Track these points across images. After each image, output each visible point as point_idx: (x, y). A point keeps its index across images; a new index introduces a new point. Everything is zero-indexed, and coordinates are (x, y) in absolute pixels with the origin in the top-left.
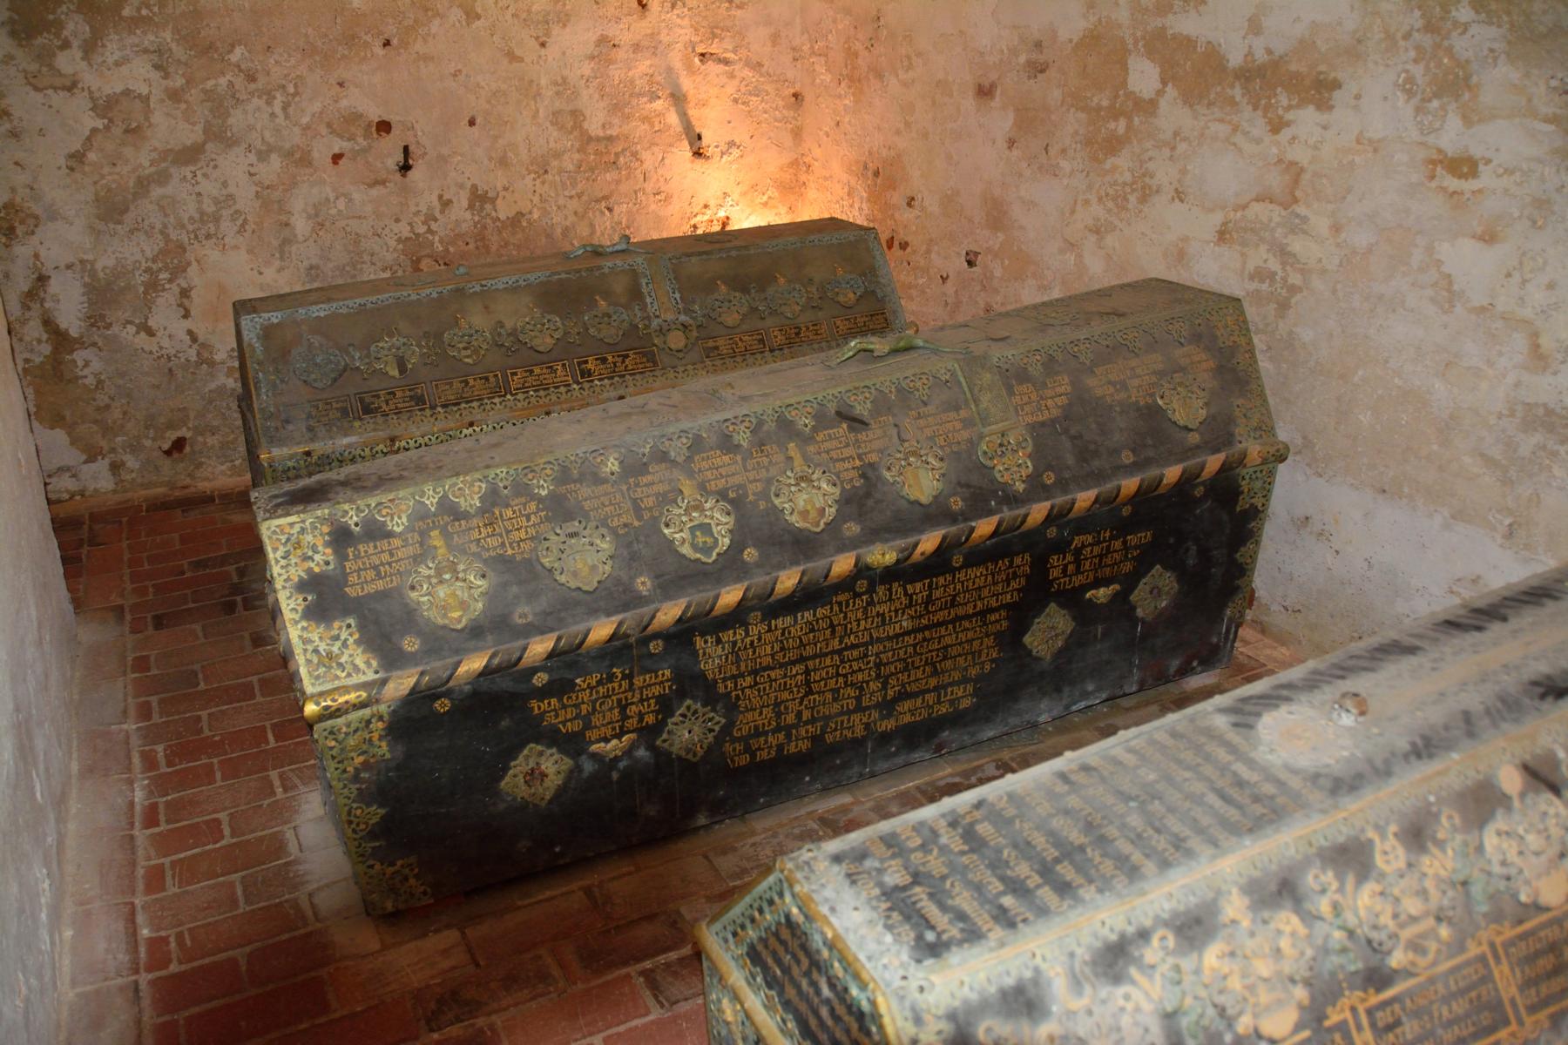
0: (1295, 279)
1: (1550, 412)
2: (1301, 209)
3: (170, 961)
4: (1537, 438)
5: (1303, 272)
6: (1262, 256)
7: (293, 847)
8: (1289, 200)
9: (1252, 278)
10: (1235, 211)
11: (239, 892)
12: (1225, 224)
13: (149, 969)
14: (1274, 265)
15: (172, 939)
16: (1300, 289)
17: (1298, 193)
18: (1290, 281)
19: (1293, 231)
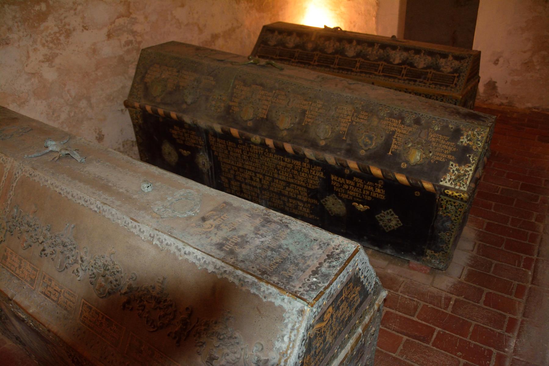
0: (139, 39)
2: (133, 16)
3: (525, 259)
6: (126, 37)
7: (465, 272)
8: (128, 14)
9: (124, 46)
10: (111, 25)
11: (492, 269)
12: (109, 31)
13: (532, 260)
14: (131, 38)
15: (522, 266)
17: (131, 11)
18: (138, 40)
19: (133, 24)
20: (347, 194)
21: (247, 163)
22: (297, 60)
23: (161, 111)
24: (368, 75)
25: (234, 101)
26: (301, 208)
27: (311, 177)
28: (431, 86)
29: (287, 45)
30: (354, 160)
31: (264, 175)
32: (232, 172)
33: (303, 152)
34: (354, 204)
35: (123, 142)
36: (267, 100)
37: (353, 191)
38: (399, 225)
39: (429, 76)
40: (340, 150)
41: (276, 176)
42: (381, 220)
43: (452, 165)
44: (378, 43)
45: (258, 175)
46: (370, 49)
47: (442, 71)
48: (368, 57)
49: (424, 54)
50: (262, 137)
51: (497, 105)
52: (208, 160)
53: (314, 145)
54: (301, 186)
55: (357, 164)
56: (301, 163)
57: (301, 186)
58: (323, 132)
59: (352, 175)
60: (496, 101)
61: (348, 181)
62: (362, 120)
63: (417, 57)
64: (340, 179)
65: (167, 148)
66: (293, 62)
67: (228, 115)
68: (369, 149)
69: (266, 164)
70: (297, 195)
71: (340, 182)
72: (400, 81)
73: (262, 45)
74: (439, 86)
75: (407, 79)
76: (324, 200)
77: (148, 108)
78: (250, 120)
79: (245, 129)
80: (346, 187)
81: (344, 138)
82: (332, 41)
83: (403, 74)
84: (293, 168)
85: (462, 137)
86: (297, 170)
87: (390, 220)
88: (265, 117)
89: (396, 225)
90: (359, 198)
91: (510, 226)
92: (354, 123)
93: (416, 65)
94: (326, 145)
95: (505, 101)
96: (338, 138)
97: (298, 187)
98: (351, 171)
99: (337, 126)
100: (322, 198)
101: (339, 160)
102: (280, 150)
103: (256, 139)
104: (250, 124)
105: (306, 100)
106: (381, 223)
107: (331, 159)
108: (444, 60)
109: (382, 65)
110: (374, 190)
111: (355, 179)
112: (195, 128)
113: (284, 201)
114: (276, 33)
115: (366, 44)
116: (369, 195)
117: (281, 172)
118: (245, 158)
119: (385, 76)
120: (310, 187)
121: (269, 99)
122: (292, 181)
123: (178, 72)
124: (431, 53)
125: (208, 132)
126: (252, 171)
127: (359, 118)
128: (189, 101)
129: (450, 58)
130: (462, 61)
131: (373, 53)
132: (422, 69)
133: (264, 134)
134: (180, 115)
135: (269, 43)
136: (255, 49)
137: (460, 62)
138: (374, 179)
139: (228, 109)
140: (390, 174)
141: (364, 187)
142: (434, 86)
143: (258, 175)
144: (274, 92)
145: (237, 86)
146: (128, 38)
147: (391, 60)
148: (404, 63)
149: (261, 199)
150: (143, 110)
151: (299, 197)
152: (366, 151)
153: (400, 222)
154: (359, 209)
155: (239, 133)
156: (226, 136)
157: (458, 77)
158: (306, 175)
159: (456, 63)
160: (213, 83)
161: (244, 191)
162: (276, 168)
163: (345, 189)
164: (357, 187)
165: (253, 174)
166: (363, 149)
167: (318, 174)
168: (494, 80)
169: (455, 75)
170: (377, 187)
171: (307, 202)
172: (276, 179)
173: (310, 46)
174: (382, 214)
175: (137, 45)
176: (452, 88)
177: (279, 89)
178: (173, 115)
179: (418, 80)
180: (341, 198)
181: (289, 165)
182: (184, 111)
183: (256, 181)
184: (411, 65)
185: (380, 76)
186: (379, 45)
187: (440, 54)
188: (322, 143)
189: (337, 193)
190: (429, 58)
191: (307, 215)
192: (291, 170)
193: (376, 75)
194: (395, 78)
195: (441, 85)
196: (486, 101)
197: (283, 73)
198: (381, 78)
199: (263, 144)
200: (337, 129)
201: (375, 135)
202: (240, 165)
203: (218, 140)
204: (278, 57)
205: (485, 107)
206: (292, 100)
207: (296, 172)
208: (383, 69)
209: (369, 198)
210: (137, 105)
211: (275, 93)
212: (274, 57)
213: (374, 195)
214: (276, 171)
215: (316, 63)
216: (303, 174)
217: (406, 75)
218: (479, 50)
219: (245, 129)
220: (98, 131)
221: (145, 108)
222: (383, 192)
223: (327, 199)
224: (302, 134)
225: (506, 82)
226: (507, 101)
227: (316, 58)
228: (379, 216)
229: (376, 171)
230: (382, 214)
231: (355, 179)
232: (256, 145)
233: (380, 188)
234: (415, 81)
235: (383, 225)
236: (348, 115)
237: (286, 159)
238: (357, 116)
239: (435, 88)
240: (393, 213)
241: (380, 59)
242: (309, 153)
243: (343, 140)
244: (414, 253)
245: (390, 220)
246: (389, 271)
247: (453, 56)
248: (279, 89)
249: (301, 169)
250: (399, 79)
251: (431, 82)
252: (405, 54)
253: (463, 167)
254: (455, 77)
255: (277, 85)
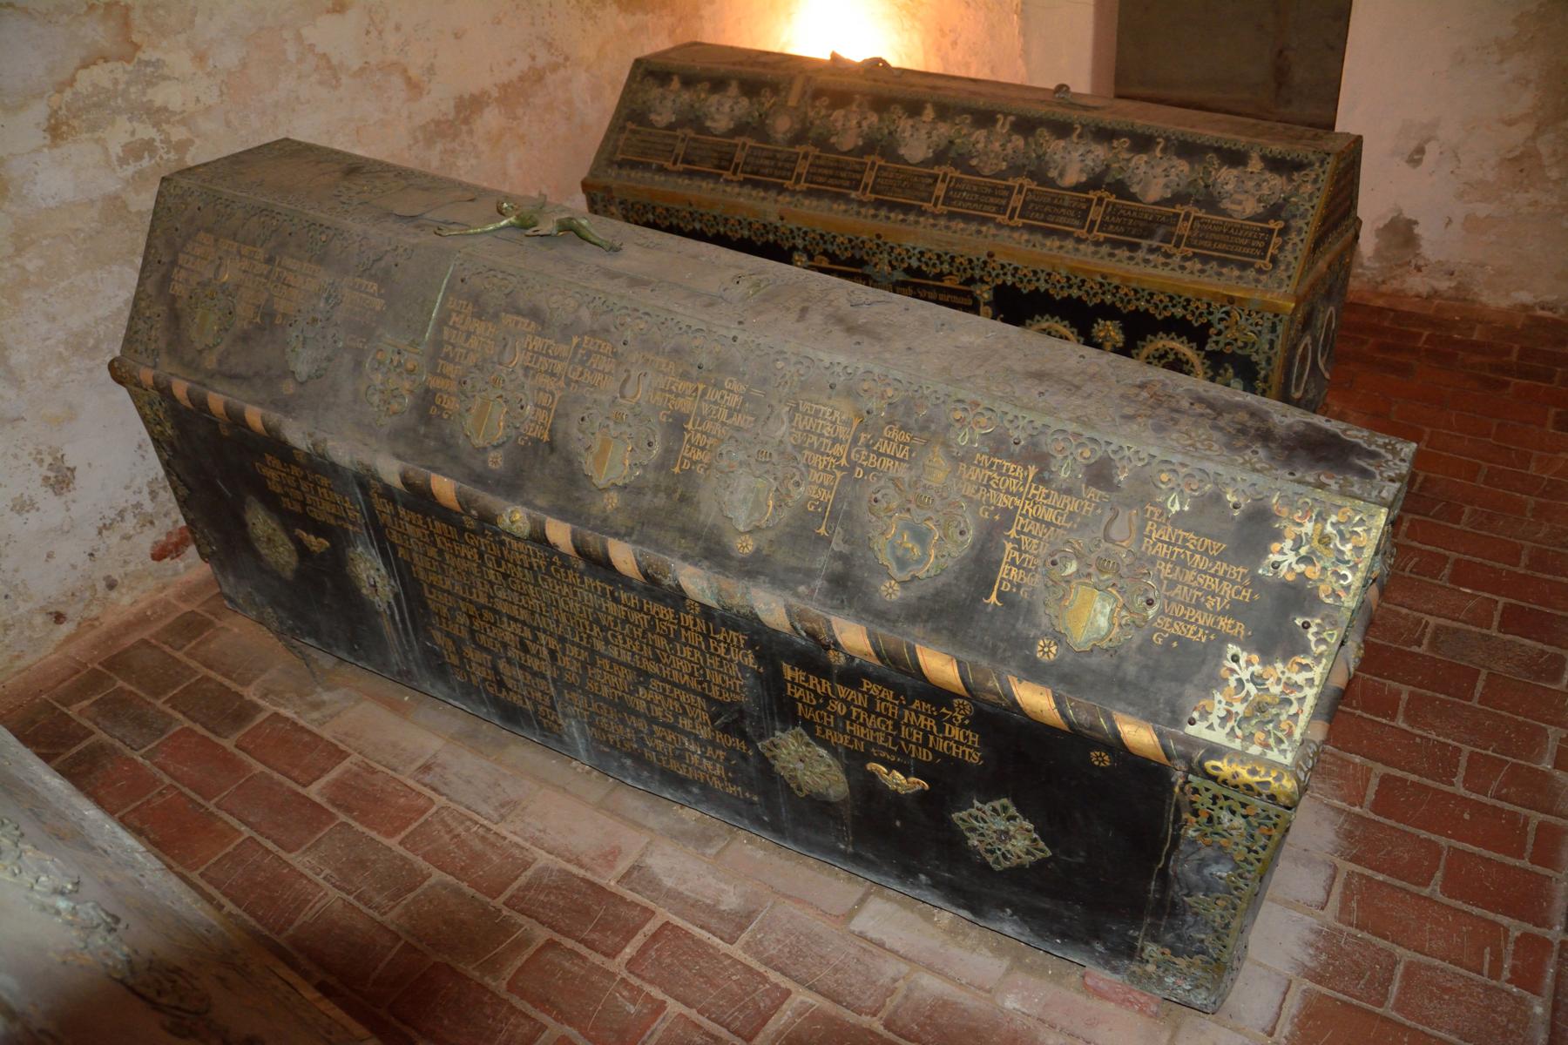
0: (178, 134)
1: (438, 123)
2: (146, 55)
3: (1518, 940)
4: (439, 147)
5: (183, 122)
6: (119, 134)
7: (1293, 1005)
8: (129, 50)
9: (123, 161)
10: (60, 92)
11: (1395, 988)
12: (54, 113)
14: (146, 132)
15: (1506, 974)
16: (190, 142)
17: (136, 38)
18: (174, 139)
19: (150, 84)
20: (844, 732)
21: (501, 594)
22: (740, 176)
23: (216, 401)
24: (973, 227)
25: (445, 376)
26: (695, 759)
27: (715, 662)
28: (1188, 264)
29: (708, 123)
30: (859, 620)
31: (562, 640)
32: (463, 619)
33: (675, 579)
34: (872, 766)
35: (150, 484)
36: (553, 375)
37: (864, 725)
38: (1040, 855)
39: (1183, 228)
40: (810, 574)
41: (600, 646)
42: (973, 830)
43: (1235, 659)
44: (1006, 115)
45: (542, 636)
46: (980, 134)
47: (1224, 212)
48: (974, 162)
49: (1164, 150)
50: (536, 514)
51: (1418, 296)
52: (383, 571)
53: (714, 553)
54: (684, 687)
55: (870, 635)
56: (676, 613)
57: (684, 687)
58: (743, 504)
59: (853, 675)
60: (1417, 284)
61: (842, 691)
62: (887, 462)
63: (1141, 160)
64: (813, 680)
65: (260, 522)
66: (728, 182)
67: (426, 422)
68: (914, 578)
69: (561, 604)
70: (676, 716)
71: (815, 692)
72: (1082, 247)
73: (630, 125)
74: (1214, 264)
75: (1107, 240)
76: (767, 743)
77: (180, 389)
78: (495, 447)
79: (479, 479)
80: (840, 709)
81: (822, 531)
82: (854, 108)
83: (1093, 223)
84: (652, 628)
85: (1276, 546)
86: (666, 636)
87: (1005, 835)
88: (546, 437)
89: (1028, 853)
90: (890, 752)
91: (1462, 791)
92: (859, 473)
93: (1135, 189)
94: (758, 550)
95: (1444, 285)
96: (802, 532)
97: (677, 691)
98: (851, 658)
99: (798, 484)
100: (761, 737)
101: (801, 615)
102: (601, 565)
103: (515, 518)
104: (496, 461)
105: (685, 376)
106: (974, 841)
107: (771, 608)
108: (1235, 172)
109: (1020, 192)
110: (941, 729)
111: (866, 685)
112: (318, 467)
113: (637, 731)
114: (676, 84)
115: (968, 119)
116: (925, 744)
117: (614, 636)
118: (492, 578)
119: (1032, 229)
120: (715, 693)
121: (559, 367)
122: (653, 668)
123: (270, 260)
124: (1188, 150)
125: (365, 481)
126: (524, 623)
127: (880, 455)
128: (302, 368)
129: (1255, 165)
130: (1295, 176)
131: (994, 148)
132: (1155, 203)
133: (540, 502)
134: (275, 417)
135: (653, 117)
136: (607, 138)
137: (1291, 180)
138: (938, 696)
139: (427, 401)
140: (994, 684)
141: (901, 717)
142: (1199, 266)
143: (542, 636)
144: (575, 340)
145: (454, 318)
146: (133, 133)
147: (1053, 174)
148: (1094, 182)
149: (565, 715)
150: (165, 391)
151: (685, 723)
152: (902, 583)
153: (1042, 844)
154: (892, 787)
155: (459, 494)
156: (419, 498)
157: (1284, 232)
158: (697, 654)
159: (1275, 184)
160: (379, 304)
161: (510, 683)
162: (597, 621)
163: (835, 714)
164: (879, 715)
165: (527, 634)
166: (892, 578)
167: (736, 657)
168: (1408, 215)
169: (1272, 225)
170: (950, 721)
171: (712, 742)
172: (603, 656)
173: (782, 125)
174: (973, 811)
175: (173, 156)
176: (1260, 271)
177: (593, 333)
178: (254, 416)
179: (1145, 243)
180: (824, 743)
181: (635, 617)
182: (285, 406)
183: (537, 655)
184: (1121, 189)
185: (1013, 229)
186: (1012, 118)
187: (1218, 150)
188: (744, 546)
189: (809, 726)
190: (1183, 166)
191: (718, 785)
192: (644, 632)
193: (1000, 226)
194: (1066, 235)
195: (1223, 262)
196: (1384, 282)
197: (616, 263)
198: (1016, 235)
199: (538, 538)
200: (798, 493)
201: (937, 524)
202: (483, 600)
203: (402, 512)
204: (680, 167)
205: (1380, 302)
206: (634, 373)
207: (661, 642)
208: (1025, 203)
209: (925, 755)
210: (146, 375)
211: (578, 346)
212: (668, 165)
213: (942, 746)
214: (596, 629)
215: (803, 186)
216: (687, 652)
217: (1104, 226)
218: (1355, 131)
219: (479, 479)
220: (48, 460)
221: (169, 388)
222: (974, 738)
223: (777, 741)
224: (670, 507)
225: (1450, 221)
226: (1453, 284)
227: (802, 168)
228: (963, 814)
229: (939, 665)
230: (973, 811)
231: (866, 685)
232: (518, 539)
233: (962, 726)
234: (1134, 247)
235: (981, 848)
236: (835, 441)
237: (624, 596)
238: (868, 446)
239: (1202, 271)
240: (1013, 811)
241: (1016, 170)
242: (695, 581)
243: (820, 538)
244: (1099, 947)
245: (1006, 833)
246: (1011, 1003)
247: (1263, 158)
248: (593, 333)
249: (677, 633)
250: (1079, 240)
251: (1190, 252)
252: (1100, 151)
253: (1279, 666)
254: (1271, 231)
255: (585, 314)
